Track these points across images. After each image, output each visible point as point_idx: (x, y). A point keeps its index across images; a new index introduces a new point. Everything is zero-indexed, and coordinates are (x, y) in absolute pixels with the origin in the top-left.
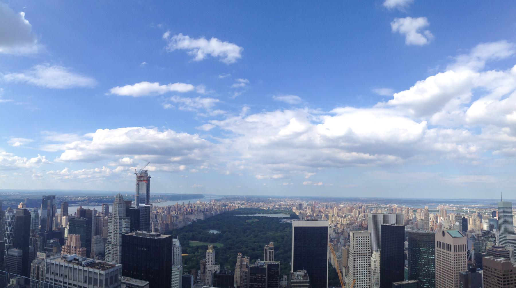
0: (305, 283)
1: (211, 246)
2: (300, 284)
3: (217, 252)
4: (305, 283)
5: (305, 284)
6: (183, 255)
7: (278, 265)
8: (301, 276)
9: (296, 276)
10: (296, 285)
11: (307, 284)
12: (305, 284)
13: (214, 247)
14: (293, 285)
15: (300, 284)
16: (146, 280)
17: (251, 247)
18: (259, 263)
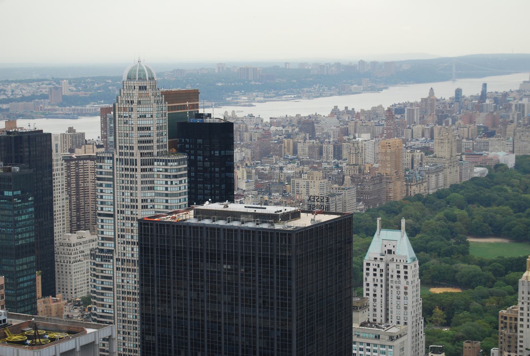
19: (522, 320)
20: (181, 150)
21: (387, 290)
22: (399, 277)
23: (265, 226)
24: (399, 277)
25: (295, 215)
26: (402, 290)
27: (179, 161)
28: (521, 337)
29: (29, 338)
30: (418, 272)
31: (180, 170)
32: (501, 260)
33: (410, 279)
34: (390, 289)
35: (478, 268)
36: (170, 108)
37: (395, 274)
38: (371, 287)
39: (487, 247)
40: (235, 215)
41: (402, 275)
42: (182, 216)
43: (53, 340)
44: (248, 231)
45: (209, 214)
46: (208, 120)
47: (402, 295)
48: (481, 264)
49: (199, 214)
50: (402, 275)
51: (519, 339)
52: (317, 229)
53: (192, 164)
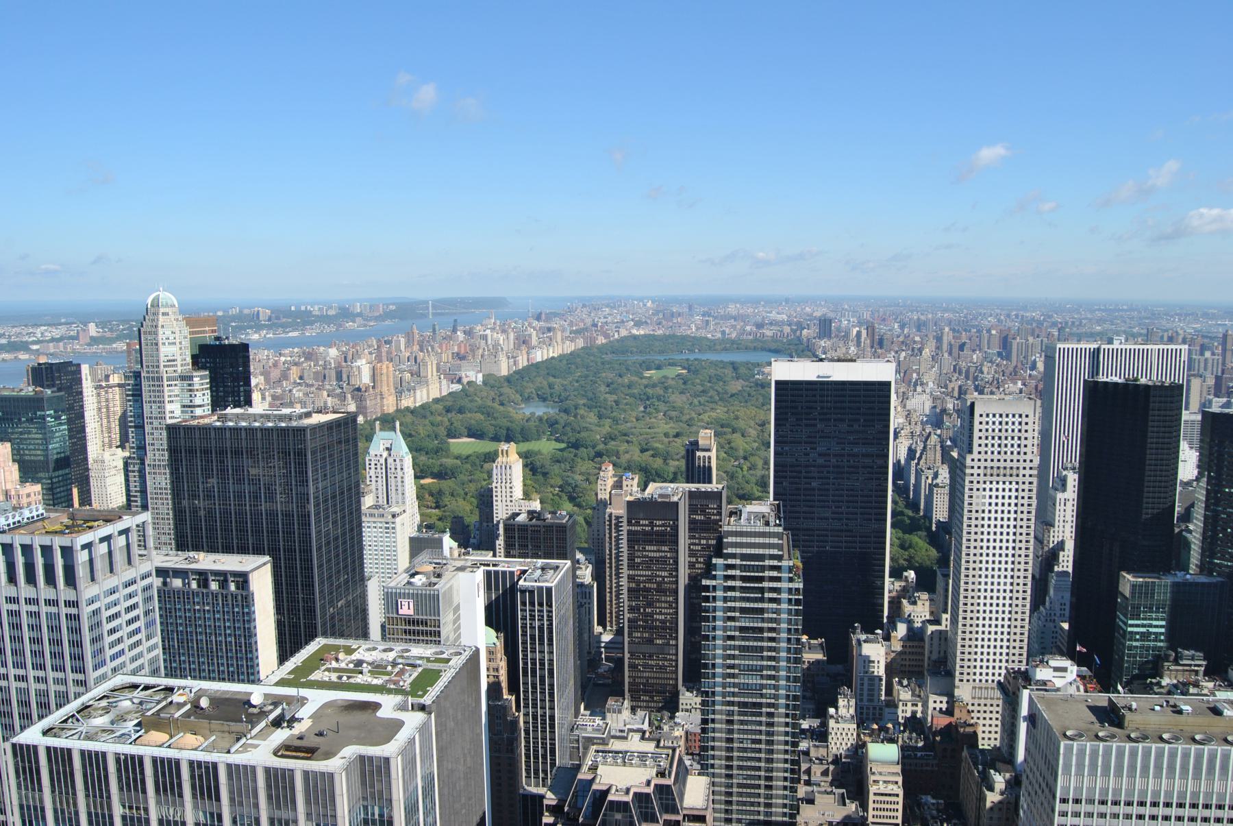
0: (770, 535)
1: (512, 447)
2: (753, 540)
3: (533, 468)
4: (770, 535)
5: (767, 540)
6: (422, 482)
7: (717, 496)
9: (744, 516)
10: (739, 540)
11: (776, 541)
12: (767, 540)
14: (730, 539)
15: (753, 540)
16: (258, 551)
17: (653, 449)
18: (654, 489)
20: (204, 368)
23: (283, 425)
25: (308, 415)
26: (399, 479)
29: (67, 527)
33: (406, 470)
35: (458, 462)
36: (191, 333)
38: (374, 479)
39: (463, 445)
40: (255, 417)
42: (207, 421)
44: (268, 429)
49: (223, 418)
52: (330, 426)
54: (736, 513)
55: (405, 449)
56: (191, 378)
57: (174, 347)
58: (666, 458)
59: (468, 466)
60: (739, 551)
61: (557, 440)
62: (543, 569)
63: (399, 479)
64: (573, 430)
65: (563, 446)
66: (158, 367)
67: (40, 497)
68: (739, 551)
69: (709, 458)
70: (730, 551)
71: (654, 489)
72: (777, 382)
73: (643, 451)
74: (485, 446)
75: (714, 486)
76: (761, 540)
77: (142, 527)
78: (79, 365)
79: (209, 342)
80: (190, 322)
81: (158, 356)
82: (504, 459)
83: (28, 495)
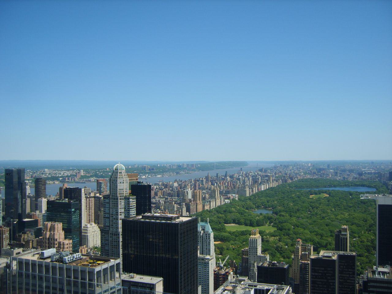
2: (382, 285)
8: (384, 273)
10: (375, 284)
13: (261, 233)
14: (371, 284)
19: (250, 252)
21: (202, 243)
22: (206, 238)
24: (206, 238)
25: (178, 218)
27: (133, 199)
28: (250, 258)
29: (90, 263)
30: (213, 236)
31: (133, 202)
32: (237, 231)
34: (203, 243)
36: (130, 180)
37: (205, 237)
39: (231, 227)
40: (157, 218)
41: (208, 237)
43: (99, 264)
45: (148, 217)
46: (142, 184)
47: (208, 245)
48: (230, 233)
50: (208, 237)
51: (249, 259)
53: (137, 199)
54: (374, 272)
55: (211, 230)
56: (129, 199)
57: (124, 187)
58: (322, 236)
59: (234, 237)
60: (375, 289)
61: (273, 226)
62: (277, 289)
63: (208, 243)
64: (279, 222)
65: (275, 229)
66: (117, 194)
67: (71, 245)
68: (375, 289)
69: (347, 239)
70: (371, 289)
71: (322, 253)
72: (380, 206)
73: (310, 232)
74: (243, 228)
75: (348, 253)
76: (386, 285)
77: (118, 265)
78: (81, 189)
79: (135, 184)
80: (129, 176)
81: (117, 190)
82: (254, 236)
83: (67, 244)
